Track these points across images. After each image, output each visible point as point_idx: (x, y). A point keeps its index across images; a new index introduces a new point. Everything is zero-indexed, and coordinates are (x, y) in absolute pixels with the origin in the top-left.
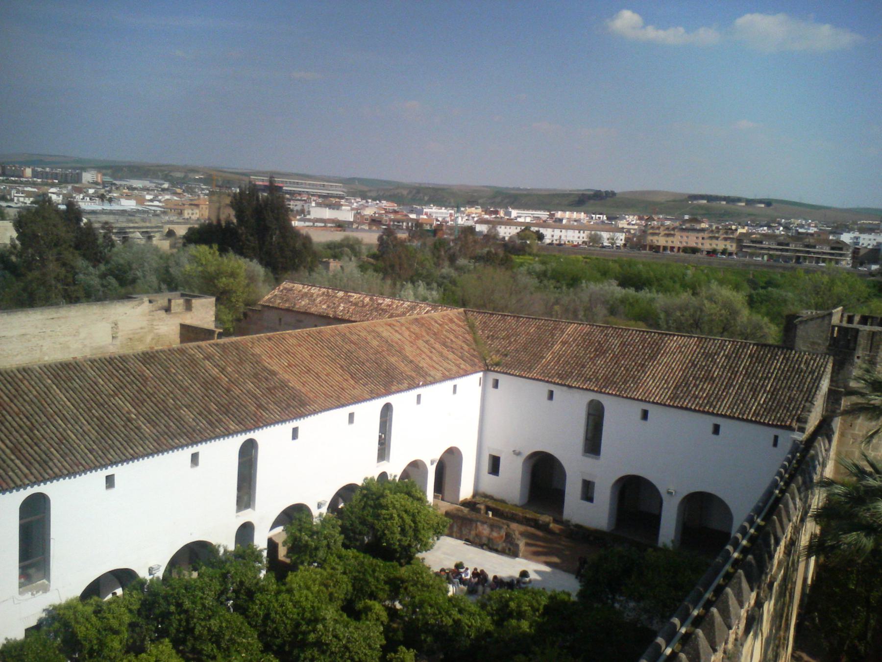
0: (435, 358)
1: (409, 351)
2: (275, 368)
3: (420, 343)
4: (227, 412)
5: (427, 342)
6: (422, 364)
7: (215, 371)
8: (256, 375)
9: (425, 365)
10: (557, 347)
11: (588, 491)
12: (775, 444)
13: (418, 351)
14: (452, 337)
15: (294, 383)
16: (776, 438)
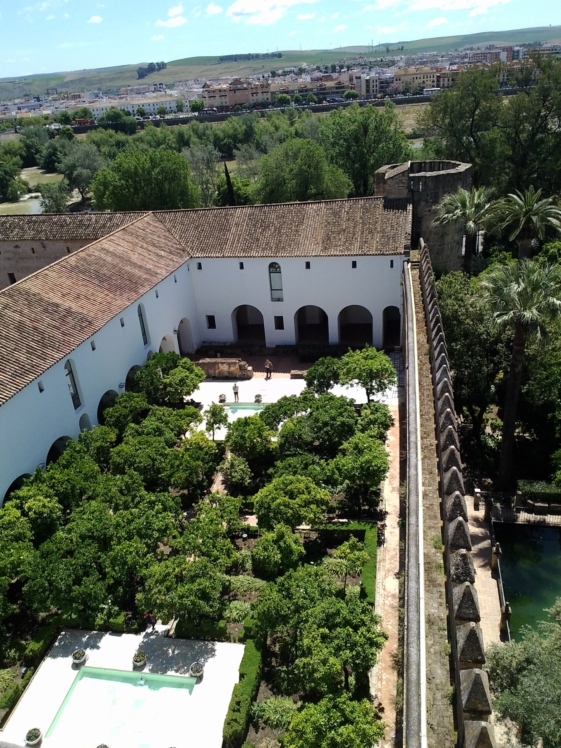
0: (154, 259)
1: (135, 258)
2: (56, 300)
3: (140, 250)
4: (45, 346)
5: (142, 247)
6: (149, 266)
7: (17, 317)
8: (46, 310)
9: (151, 267)
10: (233, 230)
11: (279, 323)
12: (392, 266)
13: (141, 257)
14: (155, 237)
15: (75, 307)
16: (392, 261)
